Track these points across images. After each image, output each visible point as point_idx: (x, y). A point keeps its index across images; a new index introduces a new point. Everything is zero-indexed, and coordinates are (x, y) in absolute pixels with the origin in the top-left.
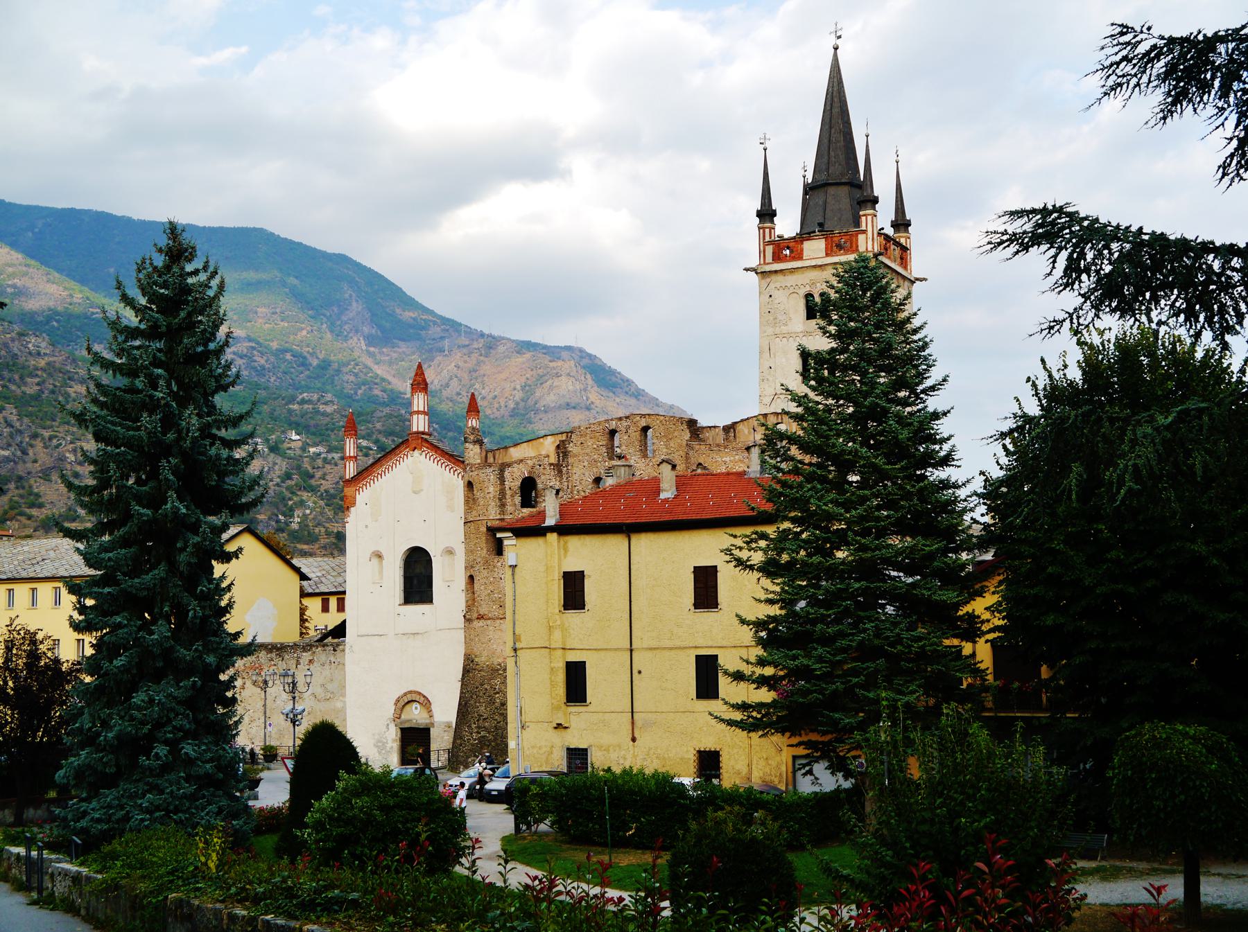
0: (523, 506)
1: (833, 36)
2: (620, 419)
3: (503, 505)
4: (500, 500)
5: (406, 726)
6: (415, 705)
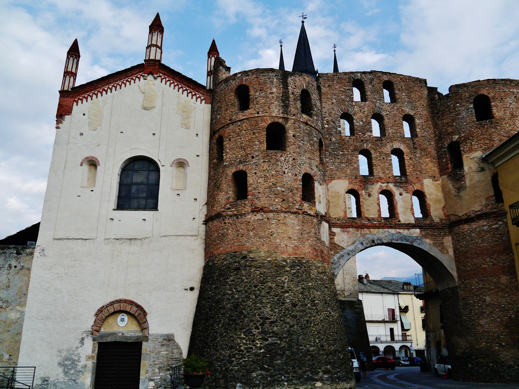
0: (303, 112)
1: (301, 18)
2: (364, 73)
3: (286, 107)
4: (283, 101)
5: (109, 339)
6: (120, 316)
